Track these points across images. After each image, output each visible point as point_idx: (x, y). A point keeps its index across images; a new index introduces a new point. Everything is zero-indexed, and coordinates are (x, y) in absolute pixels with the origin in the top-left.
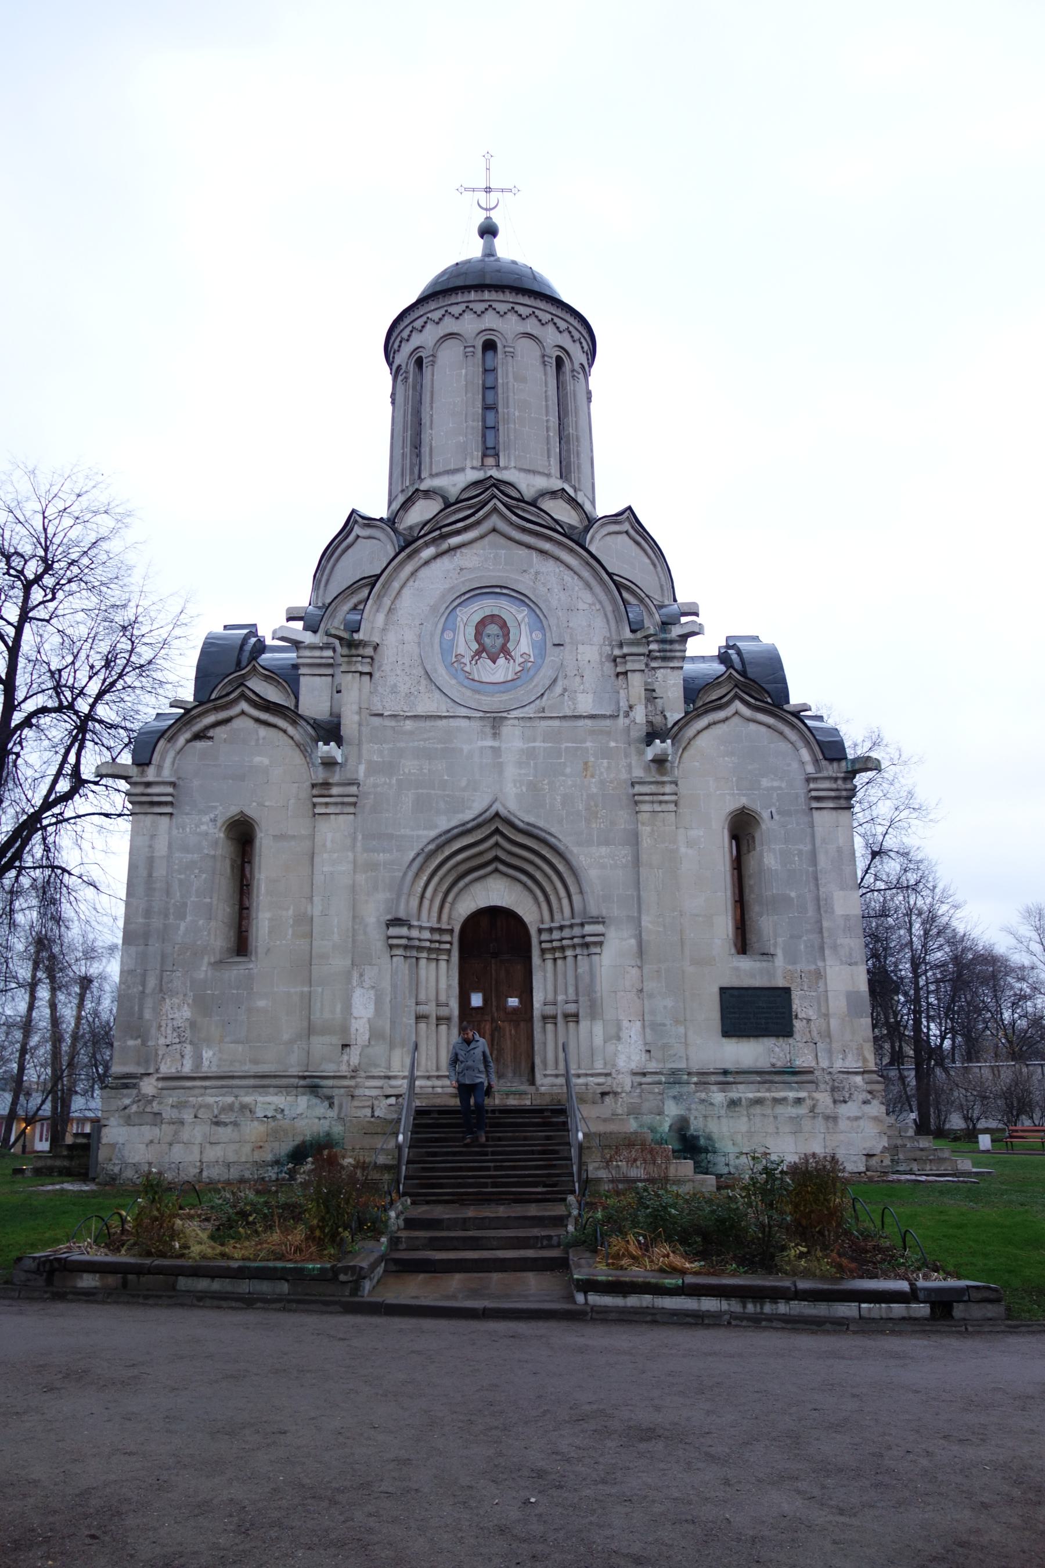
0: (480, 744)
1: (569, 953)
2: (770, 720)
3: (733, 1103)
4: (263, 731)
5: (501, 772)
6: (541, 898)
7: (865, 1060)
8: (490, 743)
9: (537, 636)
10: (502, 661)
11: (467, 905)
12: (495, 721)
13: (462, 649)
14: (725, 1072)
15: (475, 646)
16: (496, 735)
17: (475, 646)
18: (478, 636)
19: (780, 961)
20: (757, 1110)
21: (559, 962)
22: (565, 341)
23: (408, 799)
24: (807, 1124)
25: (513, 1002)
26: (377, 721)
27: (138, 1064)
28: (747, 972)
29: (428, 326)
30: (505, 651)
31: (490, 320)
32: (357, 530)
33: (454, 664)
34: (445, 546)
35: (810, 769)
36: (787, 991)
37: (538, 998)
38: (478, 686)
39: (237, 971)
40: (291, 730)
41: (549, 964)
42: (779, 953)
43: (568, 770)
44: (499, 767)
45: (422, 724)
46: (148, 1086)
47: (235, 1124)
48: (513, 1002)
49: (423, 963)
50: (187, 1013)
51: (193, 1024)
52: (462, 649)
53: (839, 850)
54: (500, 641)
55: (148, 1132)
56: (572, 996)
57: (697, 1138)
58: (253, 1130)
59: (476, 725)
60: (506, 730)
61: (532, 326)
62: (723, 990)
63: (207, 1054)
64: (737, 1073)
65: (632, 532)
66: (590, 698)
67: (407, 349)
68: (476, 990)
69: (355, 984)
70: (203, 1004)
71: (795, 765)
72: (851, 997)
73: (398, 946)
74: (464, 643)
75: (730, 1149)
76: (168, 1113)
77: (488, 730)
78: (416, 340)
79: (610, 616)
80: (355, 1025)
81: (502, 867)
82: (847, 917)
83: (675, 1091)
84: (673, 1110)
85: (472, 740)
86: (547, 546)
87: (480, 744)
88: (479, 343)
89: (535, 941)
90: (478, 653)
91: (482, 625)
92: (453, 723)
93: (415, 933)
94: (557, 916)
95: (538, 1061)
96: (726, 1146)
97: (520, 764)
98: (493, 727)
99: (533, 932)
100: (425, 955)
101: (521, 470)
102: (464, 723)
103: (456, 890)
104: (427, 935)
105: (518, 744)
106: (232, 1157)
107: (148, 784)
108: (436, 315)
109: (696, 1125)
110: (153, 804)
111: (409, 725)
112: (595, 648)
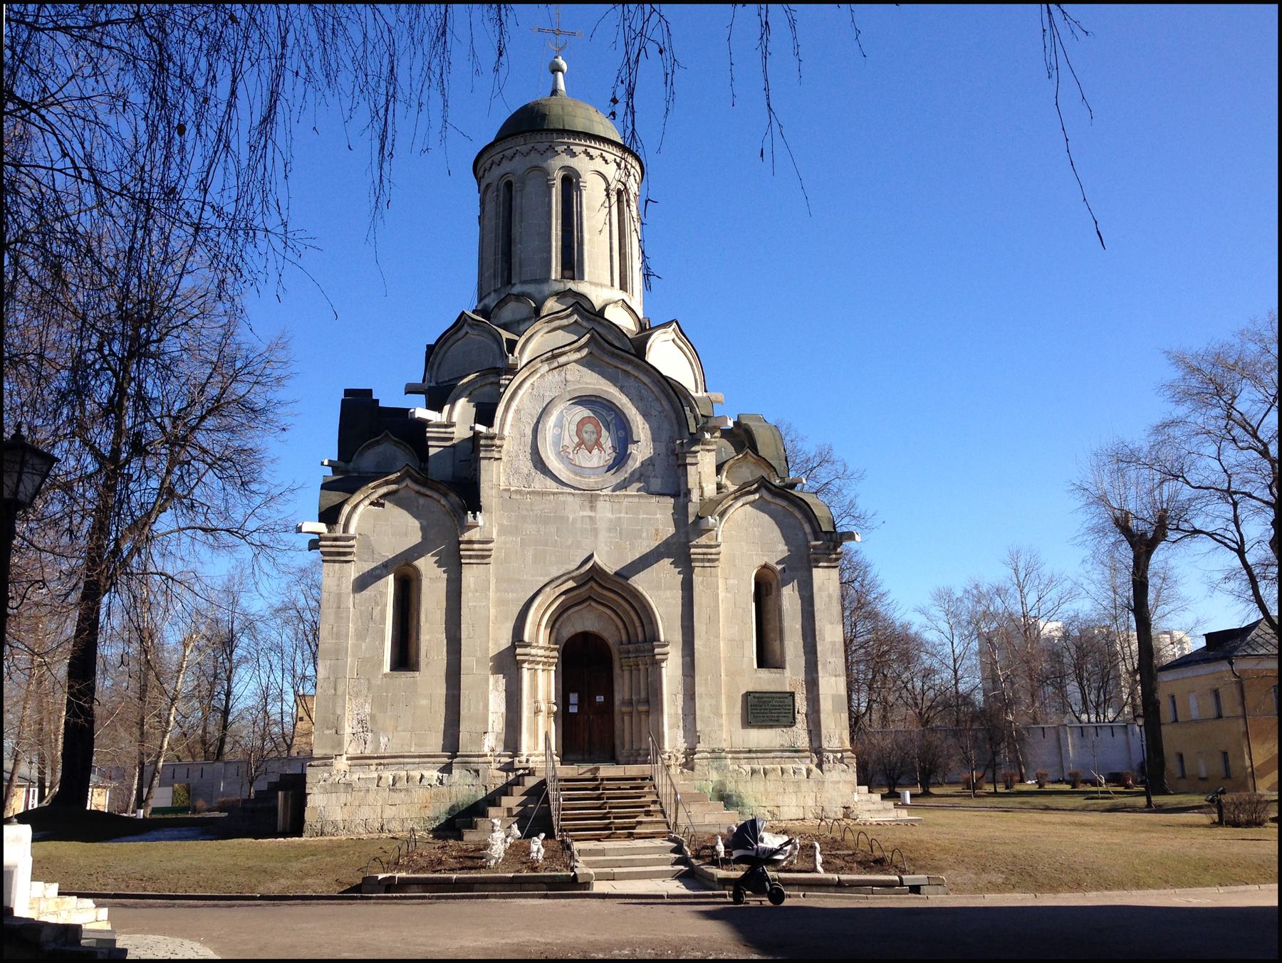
0: (581, 513)
1: (641, 667)
2: (784, 504)
3: (753, 772)
4: (422, 501)
5: (596, 536)
6: (621, 626)
7: (842, 742)
8: (588, 513)
9: (621, 433)
10: (596, 451)
11: (568, 632)
12: (591, 497)
13: (567, 441)
15: (576, 440)
16: (592, 508)
18: (578, 433)
19: (788, 672)
20: (771, 776)
21: (635, 672)
23: (529, 554)
24: (804, 787)
25: (600, 699)
26: (506, 495)
27: (333, 748)
28: (767, 681)
29: (517, 157)
30: (597, 443)
31: (567, 161)
32: (466, 328)
33: (562, 454)
34: (556, 364)
35: (810, 537)
37: (618, 698)
38: (578, 470)
39: (404, 677)
40: (443, 501)
41: (627, 674)
43: (644, 534)
44: (595, 532)
46: (342, 764)
47: (407, 790)
48: (600, 699)
49: (540, 672)
50: (368, 709)
51: (372, 717)
52: (567, 441)
54: (595, 436)
55: (343, 797)
56: (643, 695)
57: (729, 796)
58: (420, 795)
59: (578, 501)
60: (600, 504)
61: (598, 164)
62: (748, 694)
63: (383, 740)
64: (756, 752)
66: (659, 481)
67: (496, 172)
68: (574, 692)
69: (491, 688)
70: (380, 703)
71: (801, 535)
72: (835, 698)
73: (524, 661)
74: (570, 439)
76: (357, 785)
77: (587, 504)
78: (506, 166)
79: (674, 421)
80: (491, 718)
81: (593, 604)
82: (833, 643)
83: (716, 764)
85: (574, 508)
86: (629, 368)
87: (581, 513)
88: (558, 176)
89: (616, 657)
90: (579, 445)
91: (581, 423)
92: (562, 498)
93: (533, 651)
94: (633, 639)
95: (618, 742)
96: (749, 801)
98: (591, 502)
99: (614, 650)
100: (540, 666)
101: (591, 283)
102: (570, 498)
103: (561, 619)
104: (541, 652)
105: (610, 515)
106: (406, 815)
107: (336, 539)
109: (730, 787)
110: (339, 554)
111: (528, 499)
112: (663, 445)
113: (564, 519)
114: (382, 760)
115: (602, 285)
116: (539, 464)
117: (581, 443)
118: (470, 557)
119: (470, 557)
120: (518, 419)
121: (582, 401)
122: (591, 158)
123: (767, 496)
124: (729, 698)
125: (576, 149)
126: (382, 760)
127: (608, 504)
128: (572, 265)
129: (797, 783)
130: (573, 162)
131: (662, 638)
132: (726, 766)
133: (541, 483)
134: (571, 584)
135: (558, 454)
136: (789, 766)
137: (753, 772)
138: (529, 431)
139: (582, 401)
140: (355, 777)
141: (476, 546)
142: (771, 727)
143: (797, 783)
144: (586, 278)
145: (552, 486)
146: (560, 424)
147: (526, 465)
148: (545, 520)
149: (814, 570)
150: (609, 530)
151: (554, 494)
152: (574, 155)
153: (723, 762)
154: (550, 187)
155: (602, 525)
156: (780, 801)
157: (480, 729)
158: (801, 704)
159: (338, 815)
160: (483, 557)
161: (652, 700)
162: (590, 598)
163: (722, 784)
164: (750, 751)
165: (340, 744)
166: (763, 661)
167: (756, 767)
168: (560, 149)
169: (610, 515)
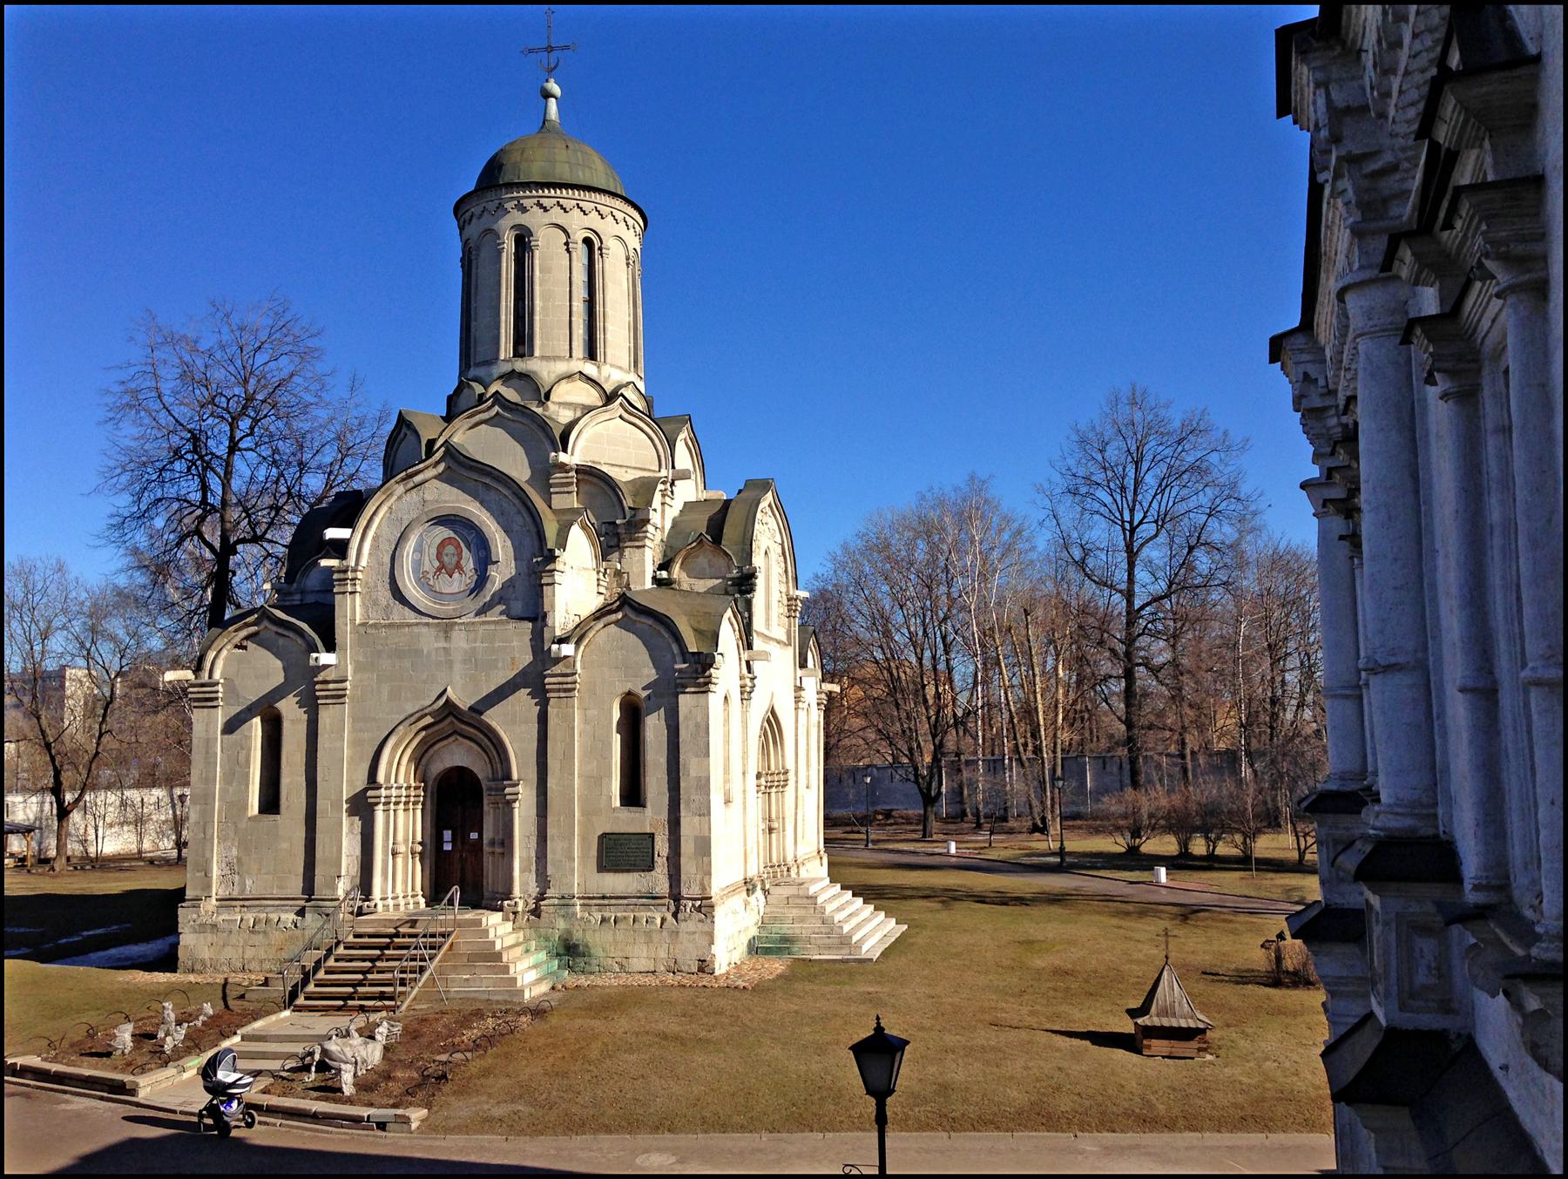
2: (650, 622)
4: (281, 641)
5: (451, 668)
8: (442, 644)
9: (482, 554)
10: (456, 575)
12: (446, 625)
13: (427, 566)
14: (604, 898)
15: (437, 564)
16: (447, 638)
17: (437, 564)
19: (649, 810)
20: (621, 925)
22: (593, 220)
24: (656, 937)
25: (474, 836)
26: (362, 630)
30: (458, 566)
33: (422, 580)
36: (652, 836)
42: (648, 805)
44: (450, 664)
45: (393, 631)
48: (474, 836)
50: (234, 852)
52: (427, 566)
53: (697, 725)
54: (455, 559)
55: (210, 937)
57: (576, 946)
58: (276, 937)
59: (432, 630)
61: (556, 215)
63: (248, 882)
65: (626, 415)
70: (245, 846)
74: (430, 564)
75: (601, 954)
76: (222, 926)
84: (561, 924)
85: (429, 640)
90: (439, 569)
91: (442, 545)
92: (415, 629)
96: (597, 952)
97: (464, 662)
99: (484, 784)
101: (543, 358)
102: (424, 630)
105: (464, 645)
107: (203, 685)
108: (476, 210)
109: (577, 936)
113: (418, 652)
114: (245, 901)
115: (556, 358)
116: (398, 594)
117: (442, 567)
118: (326, 697)
119: (326, 697)
120: (375, 546)
121: (443, 520)
122: (546, 210)
123: (632, 615)
124: (584, 839)
125: (526, 202)
126: (245, 901)
127: (463, 634)
128: (523, 342)
129: (648, 934)
130: (523, 219)
131: (515, 776)
132: (575, 914)
133: (400, 614)
134: (429, 720)
135: (418, 581)
136: (643, 915)
137: (603, 920)
138: (387, 560)
139: (443, 520)
140: (221, 918)
141: (331, 686)
142: (628, 871)
143: (648, 934)
144: (537, 353)
145: (411, 617)
146: (419, 549)
147: (385, 595)
148: (399, 654)
149: (681, 697)
150: (464, 662)
151: (409, 625)
152: (524, 210)
153: (571, 910)
154: (500, 252)
155: (457, 657)
156: (629, 951)
157: (333, 872)
158: (662, 846)
159: (206, 954)
160: (339, 697)
161: (506, 842)
162: (455, 732)
163: (569, 932)
164: (604, 898)
165: (209, 887)
166: (633, 795)
167: (607, 915)
168: (509, 205)
169: (464, 645)
